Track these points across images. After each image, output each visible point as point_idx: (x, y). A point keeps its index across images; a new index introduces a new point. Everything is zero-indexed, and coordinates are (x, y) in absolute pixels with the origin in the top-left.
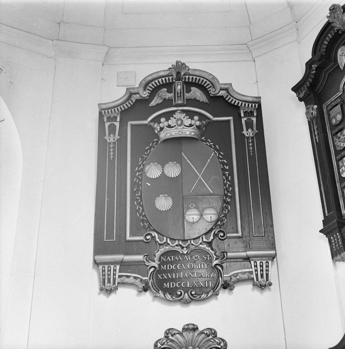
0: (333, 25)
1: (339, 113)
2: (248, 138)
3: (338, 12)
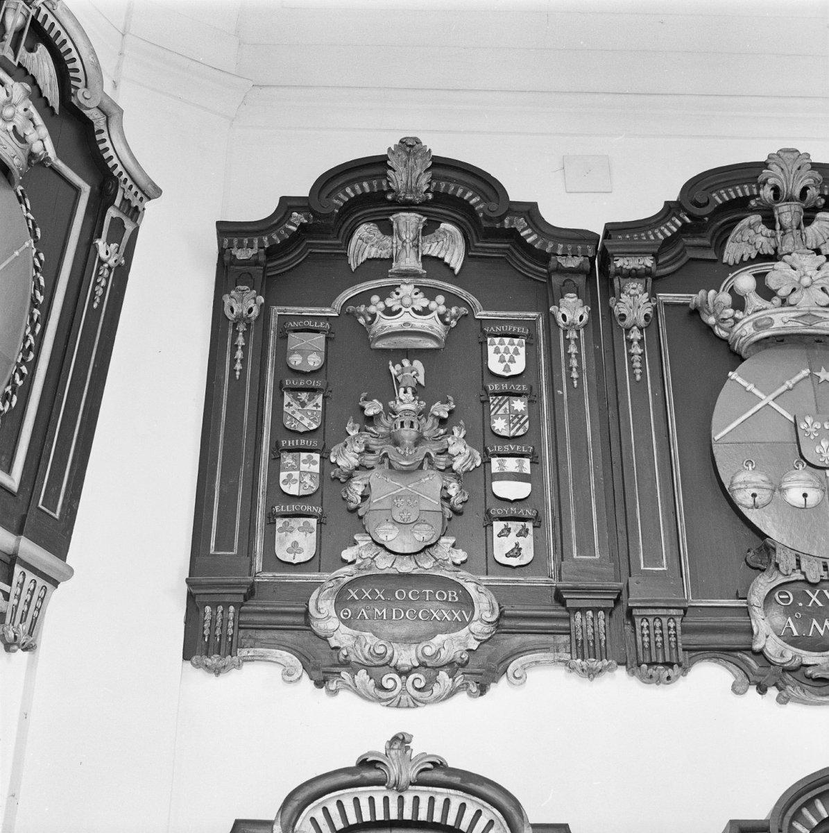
0: (390, 172)
1: (318, 352)
2: (102, 262)
3: (419, 161)
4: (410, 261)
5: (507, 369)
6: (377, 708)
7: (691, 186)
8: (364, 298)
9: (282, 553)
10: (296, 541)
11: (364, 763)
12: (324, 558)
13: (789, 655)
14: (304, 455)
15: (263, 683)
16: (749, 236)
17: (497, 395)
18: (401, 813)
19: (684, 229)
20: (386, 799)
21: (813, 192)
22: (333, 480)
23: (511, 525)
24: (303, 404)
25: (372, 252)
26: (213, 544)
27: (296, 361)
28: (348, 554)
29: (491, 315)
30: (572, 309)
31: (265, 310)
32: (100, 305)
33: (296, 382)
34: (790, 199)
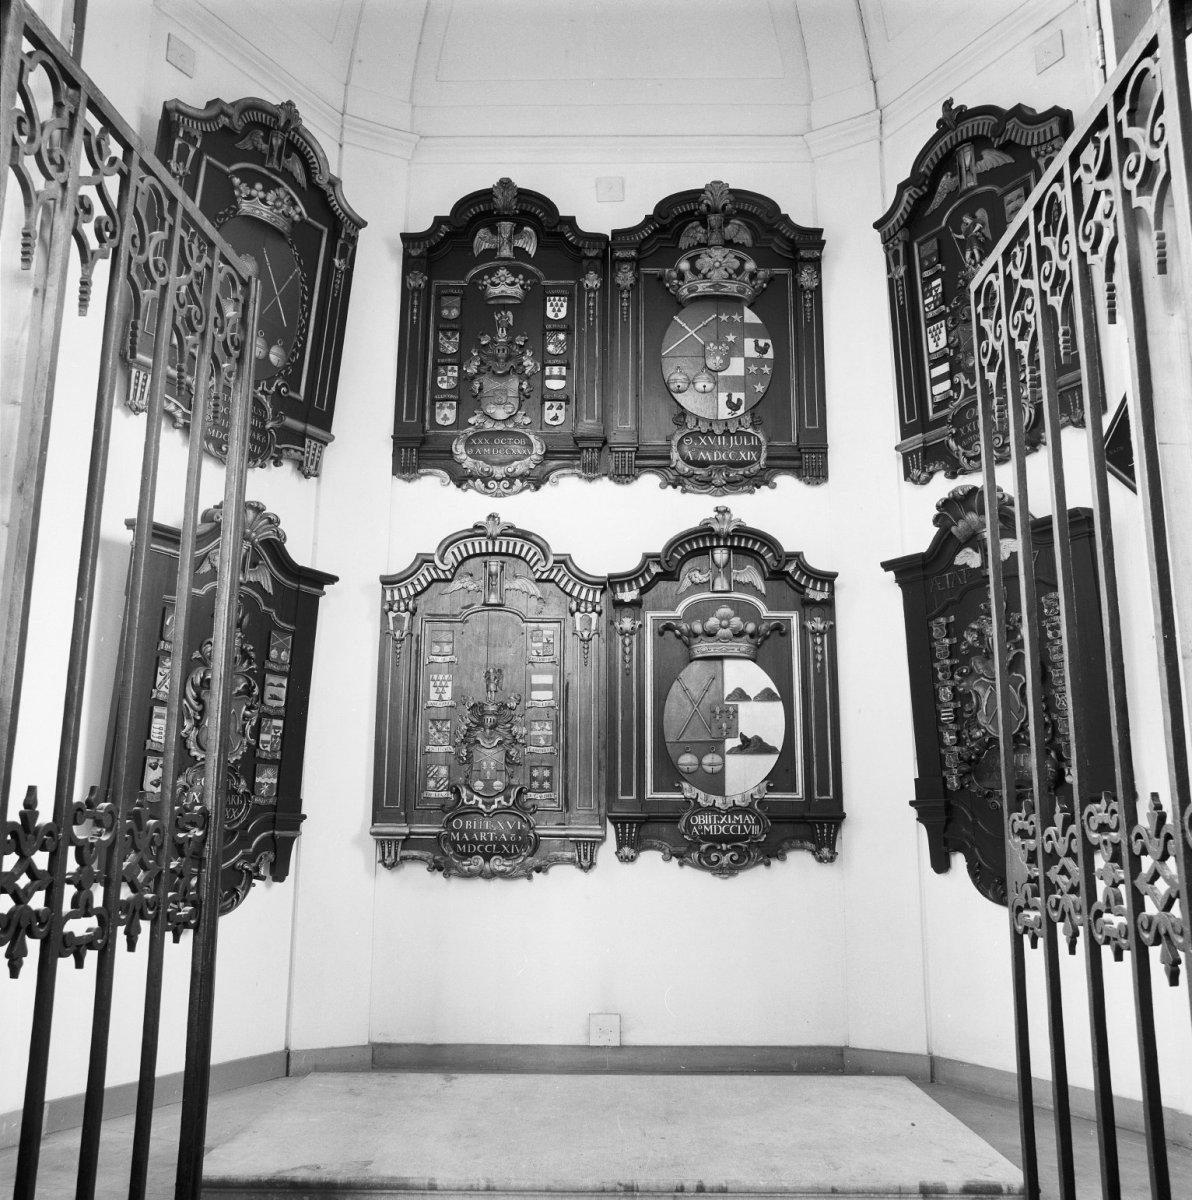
2: (337, 270)
4: (506, 252)
5: (556, 315)
6: (487, 498)
7: (660, 207)
8: (480, 276)
9: (439, 421)
10: (446, 415)
11: (476, 527)
12: (460, 423)
13: (687, 469)
14: (450, 367)
15: (432, 486)
16: (695, 233)
17: (550, 331)
18: (494, 549)
19: (656, 231)
20: (487, 543)
21: (729, 206)
22: (465, 380)
23: (554, 404)
24: (449, 339)
25: (487, 246)
26: (404, 417)
27: (445, 312)
28: (472, 420)
29: (550, 282)
30: (592, 281)
31: (428, 284)
32: (339, 294)
33: (445, 326)
34: (716, 212)
